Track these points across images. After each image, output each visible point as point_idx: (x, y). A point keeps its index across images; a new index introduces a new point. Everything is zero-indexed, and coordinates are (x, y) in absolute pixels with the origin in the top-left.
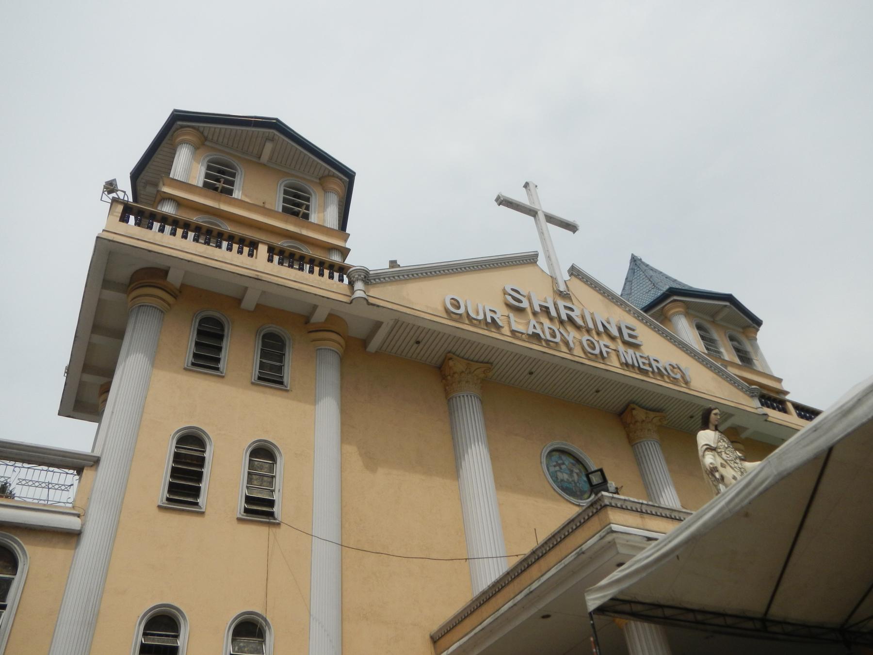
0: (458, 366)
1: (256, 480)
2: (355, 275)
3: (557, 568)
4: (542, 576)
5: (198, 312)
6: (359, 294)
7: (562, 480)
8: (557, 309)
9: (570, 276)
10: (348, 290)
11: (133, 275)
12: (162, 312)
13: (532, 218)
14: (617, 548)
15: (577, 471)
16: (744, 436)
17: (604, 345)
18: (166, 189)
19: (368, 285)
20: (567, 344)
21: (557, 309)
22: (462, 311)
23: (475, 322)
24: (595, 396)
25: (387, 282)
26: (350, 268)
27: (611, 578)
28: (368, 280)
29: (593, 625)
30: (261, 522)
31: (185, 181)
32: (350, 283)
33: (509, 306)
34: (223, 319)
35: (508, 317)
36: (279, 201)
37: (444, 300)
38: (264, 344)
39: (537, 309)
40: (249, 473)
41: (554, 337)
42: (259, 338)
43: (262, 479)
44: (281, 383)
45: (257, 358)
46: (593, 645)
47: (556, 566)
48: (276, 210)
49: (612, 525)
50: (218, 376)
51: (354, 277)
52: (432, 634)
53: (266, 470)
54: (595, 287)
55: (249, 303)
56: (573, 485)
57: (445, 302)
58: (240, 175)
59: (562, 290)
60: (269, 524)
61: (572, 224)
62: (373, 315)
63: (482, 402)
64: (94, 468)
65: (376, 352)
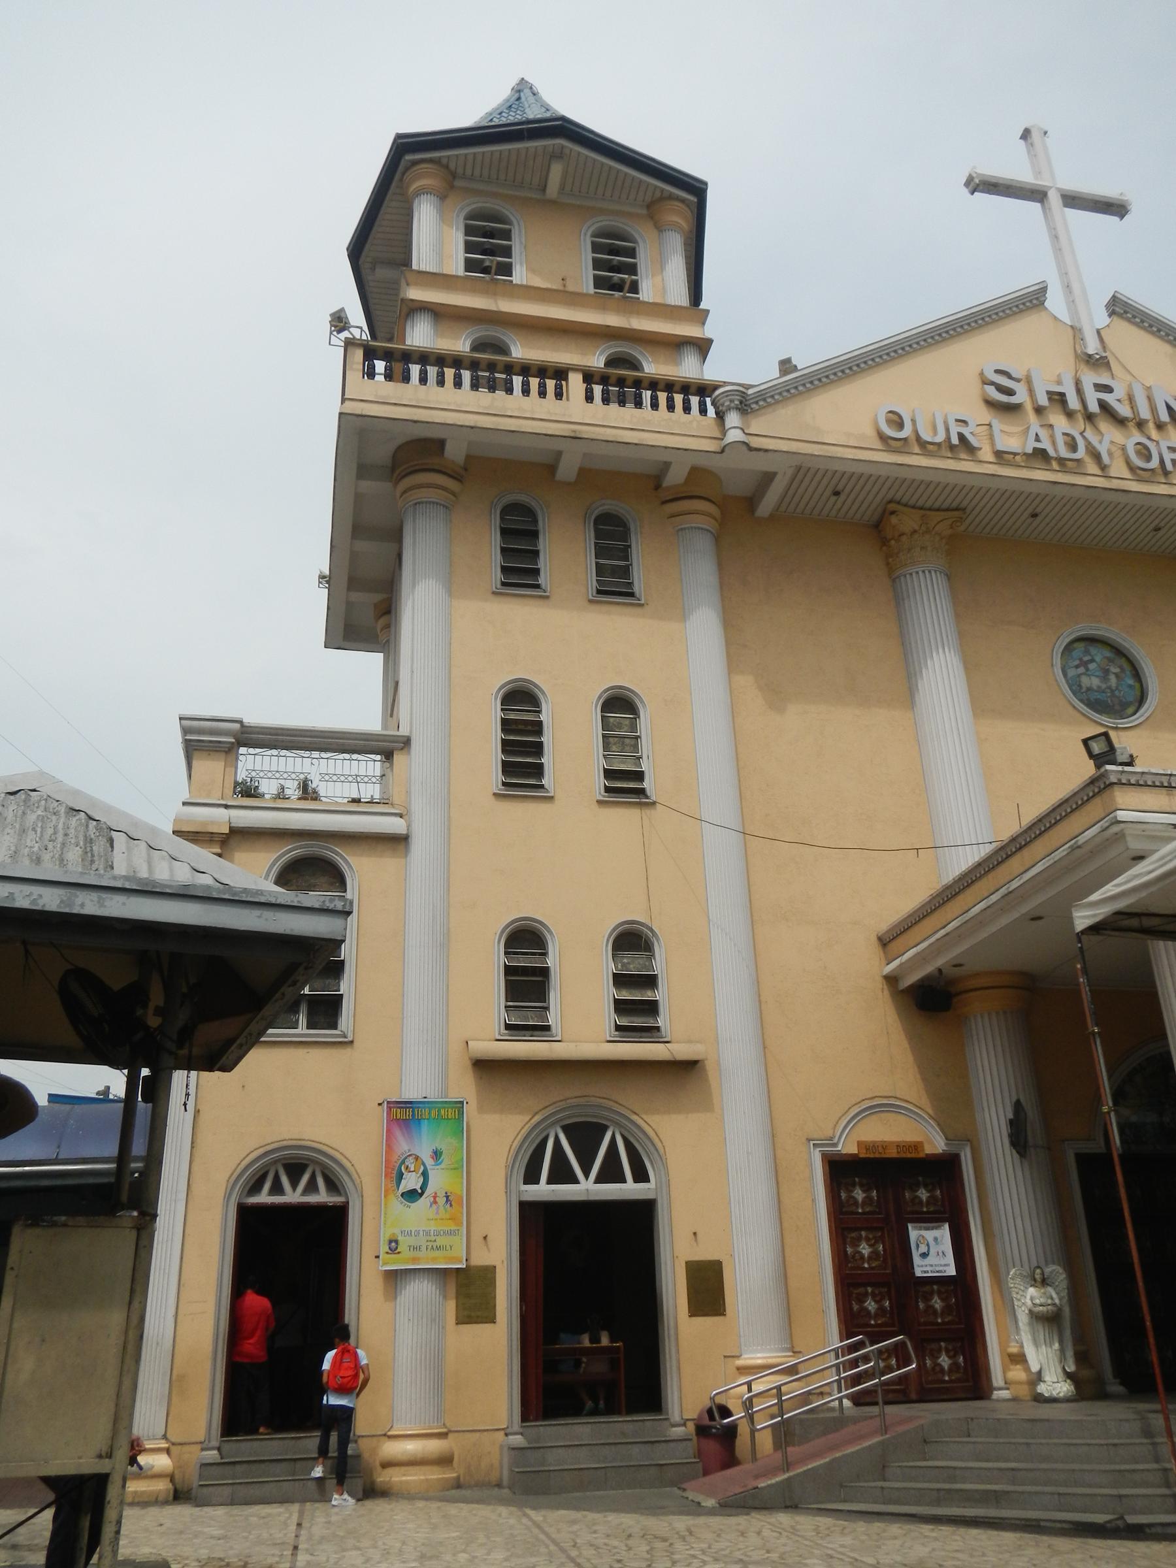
0: (907, 522)
1: (615, 744)
2: (725, 401)
3: (1044, 864)
4: (1025, 871)
5: (496, 500)
6: (734, 435)
7: (1089, 689)
8: (1079, 391)
9: (1110, 316)
10: (716, 428)
11: (394, 456)
12: (447, 507)
13: (1038, 205)
14: (1126, 842)
15: (1117, 670)
17: (1169, 448)
18: (415, 293)
19: (747, 414)
20: (1096, 456)
21: (1079, 391)
22: (907, 432)
23: (930, 447)
24: (1154, 536)
25: (777, 402)
26: (716, 388)
27: (1105, 893)
28: (745, 405)
29: (1081, 948)
30: (630, 803)
31: (438, 272)
32: (717, 413)
33: (990, 404)
34: (533, 504)
35: (990, 425)
36: (586, 269)
37: (876, 415)
38: (599, 534)
39: (1043, 400)
40: (604, 736)
41: (1073, 447)
42: (589, 523)
43: (623, 743)
44: (632, 595)
45: (591, 560)
46: (1080, 973)
47: (1049, 858)
48: (585, 291)
49: (1119, 812)
50: (541, 597)
51: (723, 405)
52: (879, 935)
53: (626, 729)
54: (1159, 331)
55: (567, 470)
56: (1109, 694)
57: (877, 419)
58: (517, 232)
59: (1090, 352)
60: (640, 804)
61: (1118, 202)
62: (761, 464)
63: (949, 577)
64: (406, 749)
65: (771, 515)
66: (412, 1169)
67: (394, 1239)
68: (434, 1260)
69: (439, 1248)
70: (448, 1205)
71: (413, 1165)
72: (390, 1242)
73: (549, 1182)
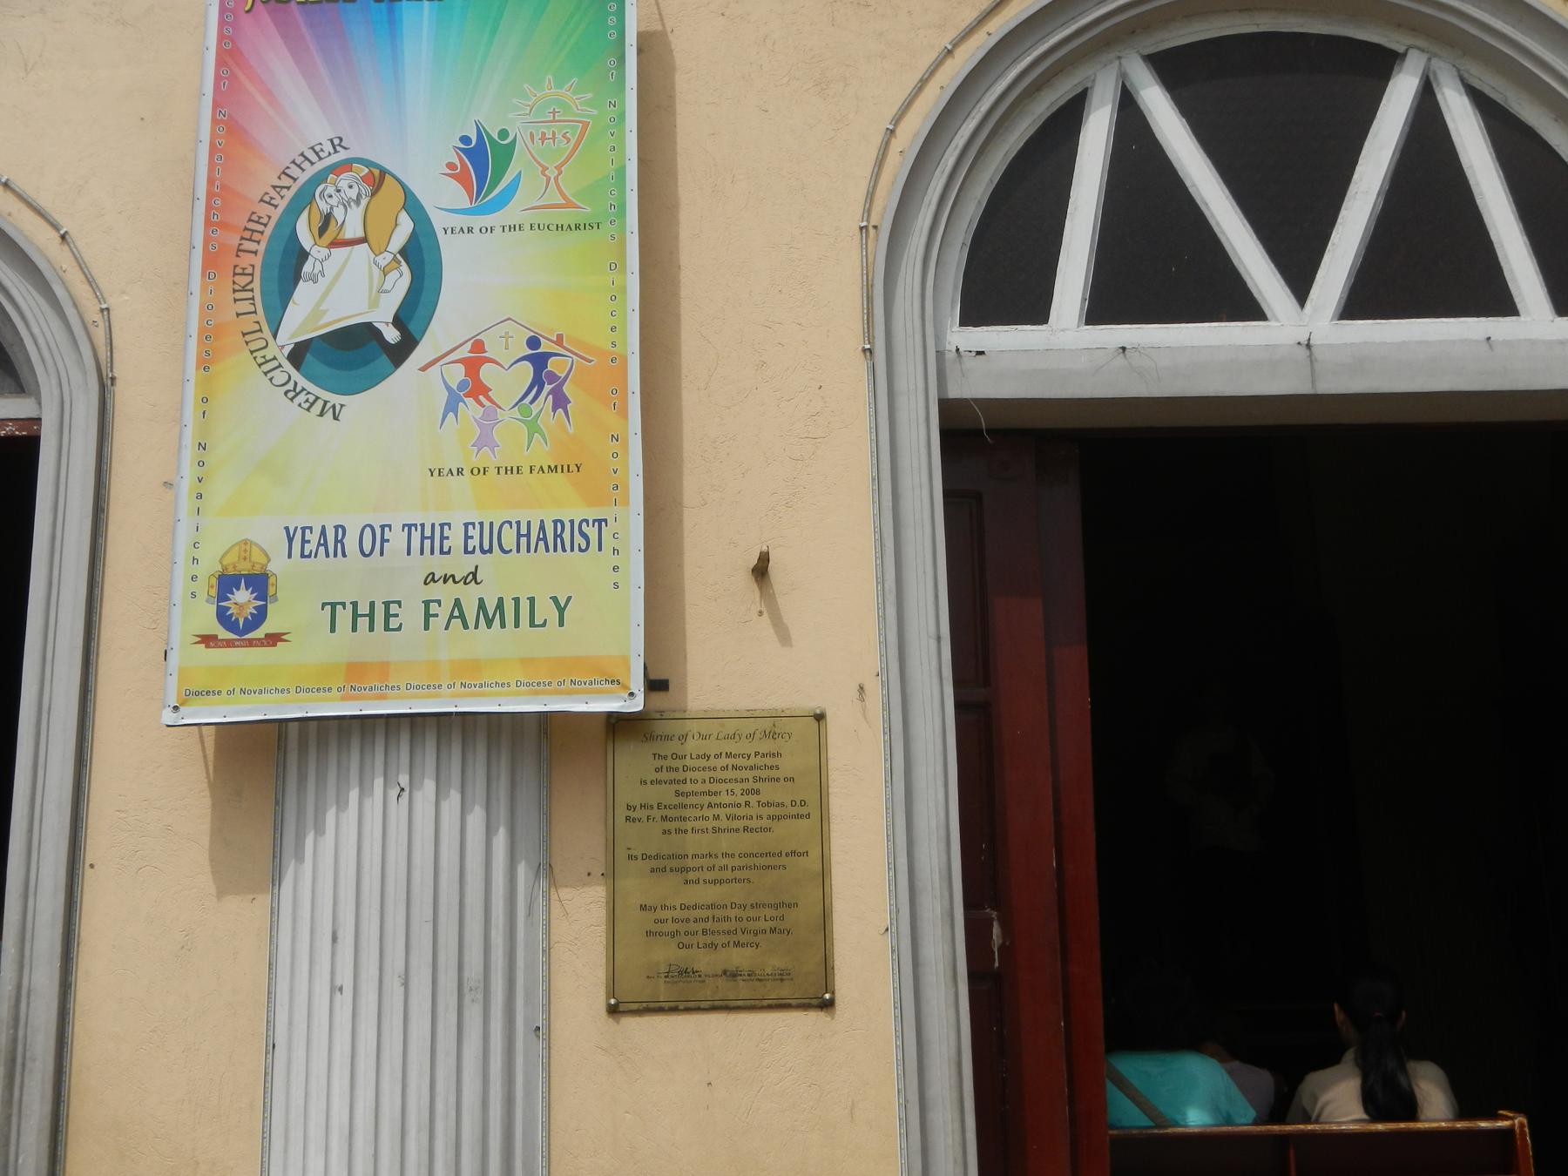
66: (353, 230)
67: (244, 568)
68: (468, 673)
69: (492, 615)
70: (545, 401)
71: (355, 215)
72: (227, 584)
73: (1101, 309)
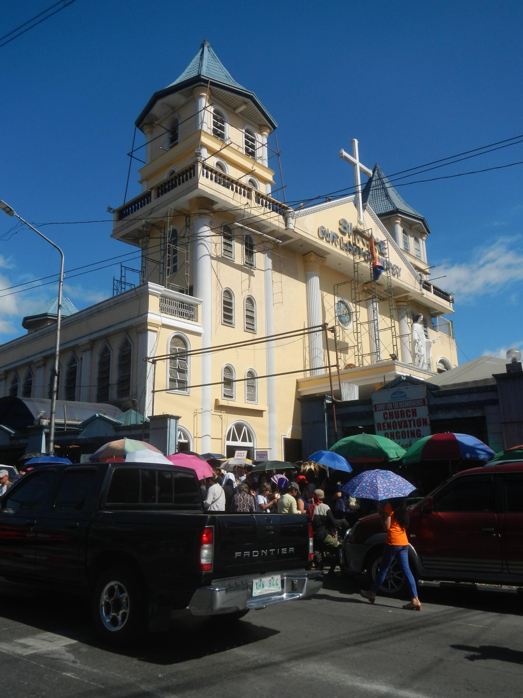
16: (409, 299)
